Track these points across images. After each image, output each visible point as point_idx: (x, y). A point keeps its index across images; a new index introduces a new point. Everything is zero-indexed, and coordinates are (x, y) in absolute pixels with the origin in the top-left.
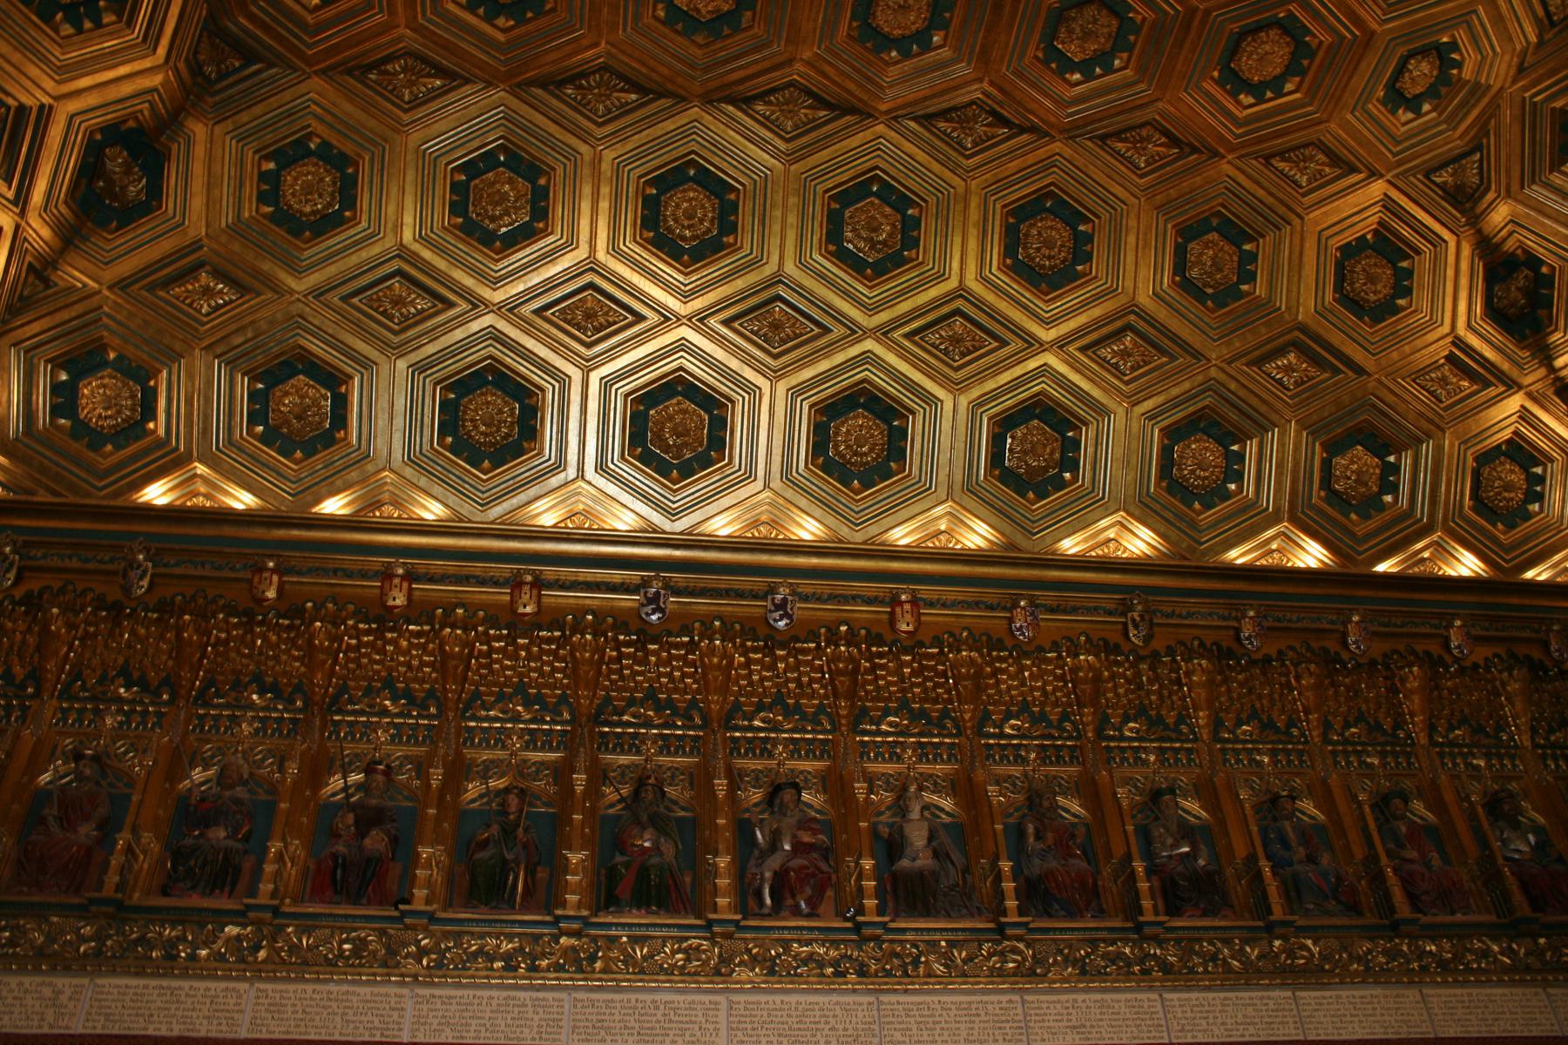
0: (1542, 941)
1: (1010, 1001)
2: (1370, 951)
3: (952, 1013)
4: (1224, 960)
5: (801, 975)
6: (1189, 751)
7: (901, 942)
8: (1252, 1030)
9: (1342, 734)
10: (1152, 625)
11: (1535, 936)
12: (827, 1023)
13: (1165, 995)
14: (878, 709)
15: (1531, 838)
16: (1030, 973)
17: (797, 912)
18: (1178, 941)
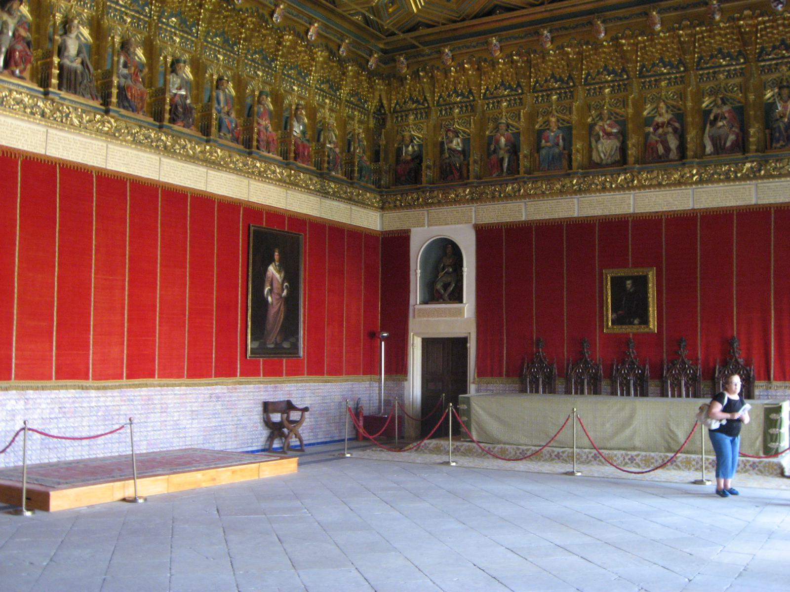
0: (293, 172)
1: (102, 146)
2: (137, 132)
4: (71, 118)
6: (193, 42)
8: (189, 183)
11: (291, 169)
12: (24, 137)
13: (162, 159)
16: (112, 135)
17: (13, 74)
18: (173, 136)
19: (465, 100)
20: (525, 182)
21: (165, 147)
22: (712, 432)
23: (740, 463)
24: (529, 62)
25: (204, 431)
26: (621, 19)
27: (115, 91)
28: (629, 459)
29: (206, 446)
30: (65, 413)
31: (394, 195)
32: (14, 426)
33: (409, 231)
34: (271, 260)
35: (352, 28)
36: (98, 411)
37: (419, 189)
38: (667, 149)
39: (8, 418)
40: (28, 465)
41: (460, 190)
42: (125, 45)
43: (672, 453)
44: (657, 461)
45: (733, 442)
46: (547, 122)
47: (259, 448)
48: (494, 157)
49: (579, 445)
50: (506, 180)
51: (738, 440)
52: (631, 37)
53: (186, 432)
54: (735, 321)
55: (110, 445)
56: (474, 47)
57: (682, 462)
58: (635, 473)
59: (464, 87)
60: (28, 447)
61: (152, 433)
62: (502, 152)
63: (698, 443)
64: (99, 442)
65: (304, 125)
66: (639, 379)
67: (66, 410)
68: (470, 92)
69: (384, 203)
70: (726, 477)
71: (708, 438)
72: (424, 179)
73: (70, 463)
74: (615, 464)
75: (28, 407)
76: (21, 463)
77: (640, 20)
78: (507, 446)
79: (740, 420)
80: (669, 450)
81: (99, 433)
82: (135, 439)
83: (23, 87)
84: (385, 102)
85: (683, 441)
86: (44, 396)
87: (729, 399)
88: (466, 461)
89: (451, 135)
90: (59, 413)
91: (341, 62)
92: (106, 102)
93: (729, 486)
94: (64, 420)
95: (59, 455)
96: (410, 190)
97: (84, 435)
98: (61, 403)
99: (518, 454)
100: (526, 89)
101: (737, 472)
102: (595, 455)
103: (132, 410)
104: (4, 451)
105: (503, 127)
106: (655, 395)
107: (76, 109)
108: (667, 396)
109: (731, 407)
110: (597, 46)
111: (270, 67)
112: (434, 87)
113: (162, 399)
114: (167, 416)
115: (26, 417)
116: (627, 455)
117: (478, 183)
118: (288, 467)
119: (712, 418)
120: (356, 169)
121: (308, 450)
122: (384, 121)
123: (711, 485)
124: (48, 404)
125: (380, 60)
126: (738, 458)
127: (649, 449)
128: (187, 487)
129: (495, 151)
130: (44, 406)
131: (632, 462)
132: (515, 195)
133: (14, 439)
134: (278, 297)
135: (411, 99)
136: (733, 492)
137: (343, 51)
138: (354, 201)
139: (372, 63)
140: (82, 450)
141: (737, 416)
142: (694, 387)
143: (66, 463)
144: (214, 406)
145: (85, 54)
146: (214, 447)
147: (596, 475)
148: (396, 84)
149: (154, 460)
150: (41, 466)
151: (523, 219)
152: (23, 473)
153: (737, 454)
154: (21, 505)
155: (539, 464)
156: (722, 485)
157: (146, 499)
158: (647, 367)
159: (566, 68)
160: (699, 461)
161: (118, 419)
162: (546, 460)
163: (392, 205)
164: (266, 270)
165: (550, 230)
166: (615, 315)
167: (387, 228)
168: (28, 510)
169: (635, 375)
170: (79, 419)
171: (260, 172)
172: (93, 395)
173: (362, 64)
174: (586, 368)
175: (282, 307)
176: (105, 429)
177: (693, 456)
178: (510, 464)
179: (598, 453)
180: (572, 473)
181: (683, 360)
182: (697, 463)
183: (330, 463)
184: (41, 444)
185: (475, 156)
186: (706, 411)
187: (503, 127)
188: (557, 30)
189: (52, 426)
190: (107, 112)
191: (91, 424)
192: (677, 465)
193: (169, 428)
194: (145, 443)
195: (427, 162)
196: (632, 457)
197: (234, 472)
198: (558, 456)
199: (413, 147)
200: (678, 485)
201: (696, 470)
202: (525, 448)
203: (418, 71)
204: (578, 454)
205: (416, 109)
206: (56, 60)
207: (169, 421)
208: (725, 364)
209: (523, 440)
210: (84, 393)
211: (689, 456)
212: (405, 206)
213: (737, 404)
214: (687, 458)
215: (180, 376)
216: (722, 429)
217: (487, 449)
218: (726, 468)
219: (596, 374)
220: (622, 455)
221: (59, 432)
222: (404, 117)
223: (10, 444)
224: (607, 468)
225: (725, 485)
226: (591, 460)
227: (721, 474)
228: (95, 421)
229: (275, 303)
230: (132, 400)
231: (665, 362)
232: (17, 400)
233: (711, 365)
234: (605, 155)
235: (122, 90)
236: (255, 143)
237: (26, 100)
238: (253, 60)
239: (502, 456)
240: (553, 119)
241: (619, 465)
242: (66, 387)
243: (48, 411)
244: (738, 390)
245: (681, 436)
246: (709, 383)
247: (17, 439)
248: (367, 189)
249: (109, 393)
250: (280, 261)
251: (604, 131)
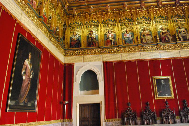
20: (121, 48)
31: (70, 51)
34: (27, 57)
38: (169, 39)
41: (97, 50)
46: (126, 31)
84: (67, 23)
129: (108, 38)
132: (117, 52)
134: (28, 77)
151: (121, 60)
163: (69, 54)
164: (24, 62)
165: (131, 64)
166: (159, 93)
167: (67, 62)
175: (29, 84)
187: (110, 31)
212: (74, 55)
229: (26, 80)
234: (148, 40)
250: (31, 59)
251: (146, 34)
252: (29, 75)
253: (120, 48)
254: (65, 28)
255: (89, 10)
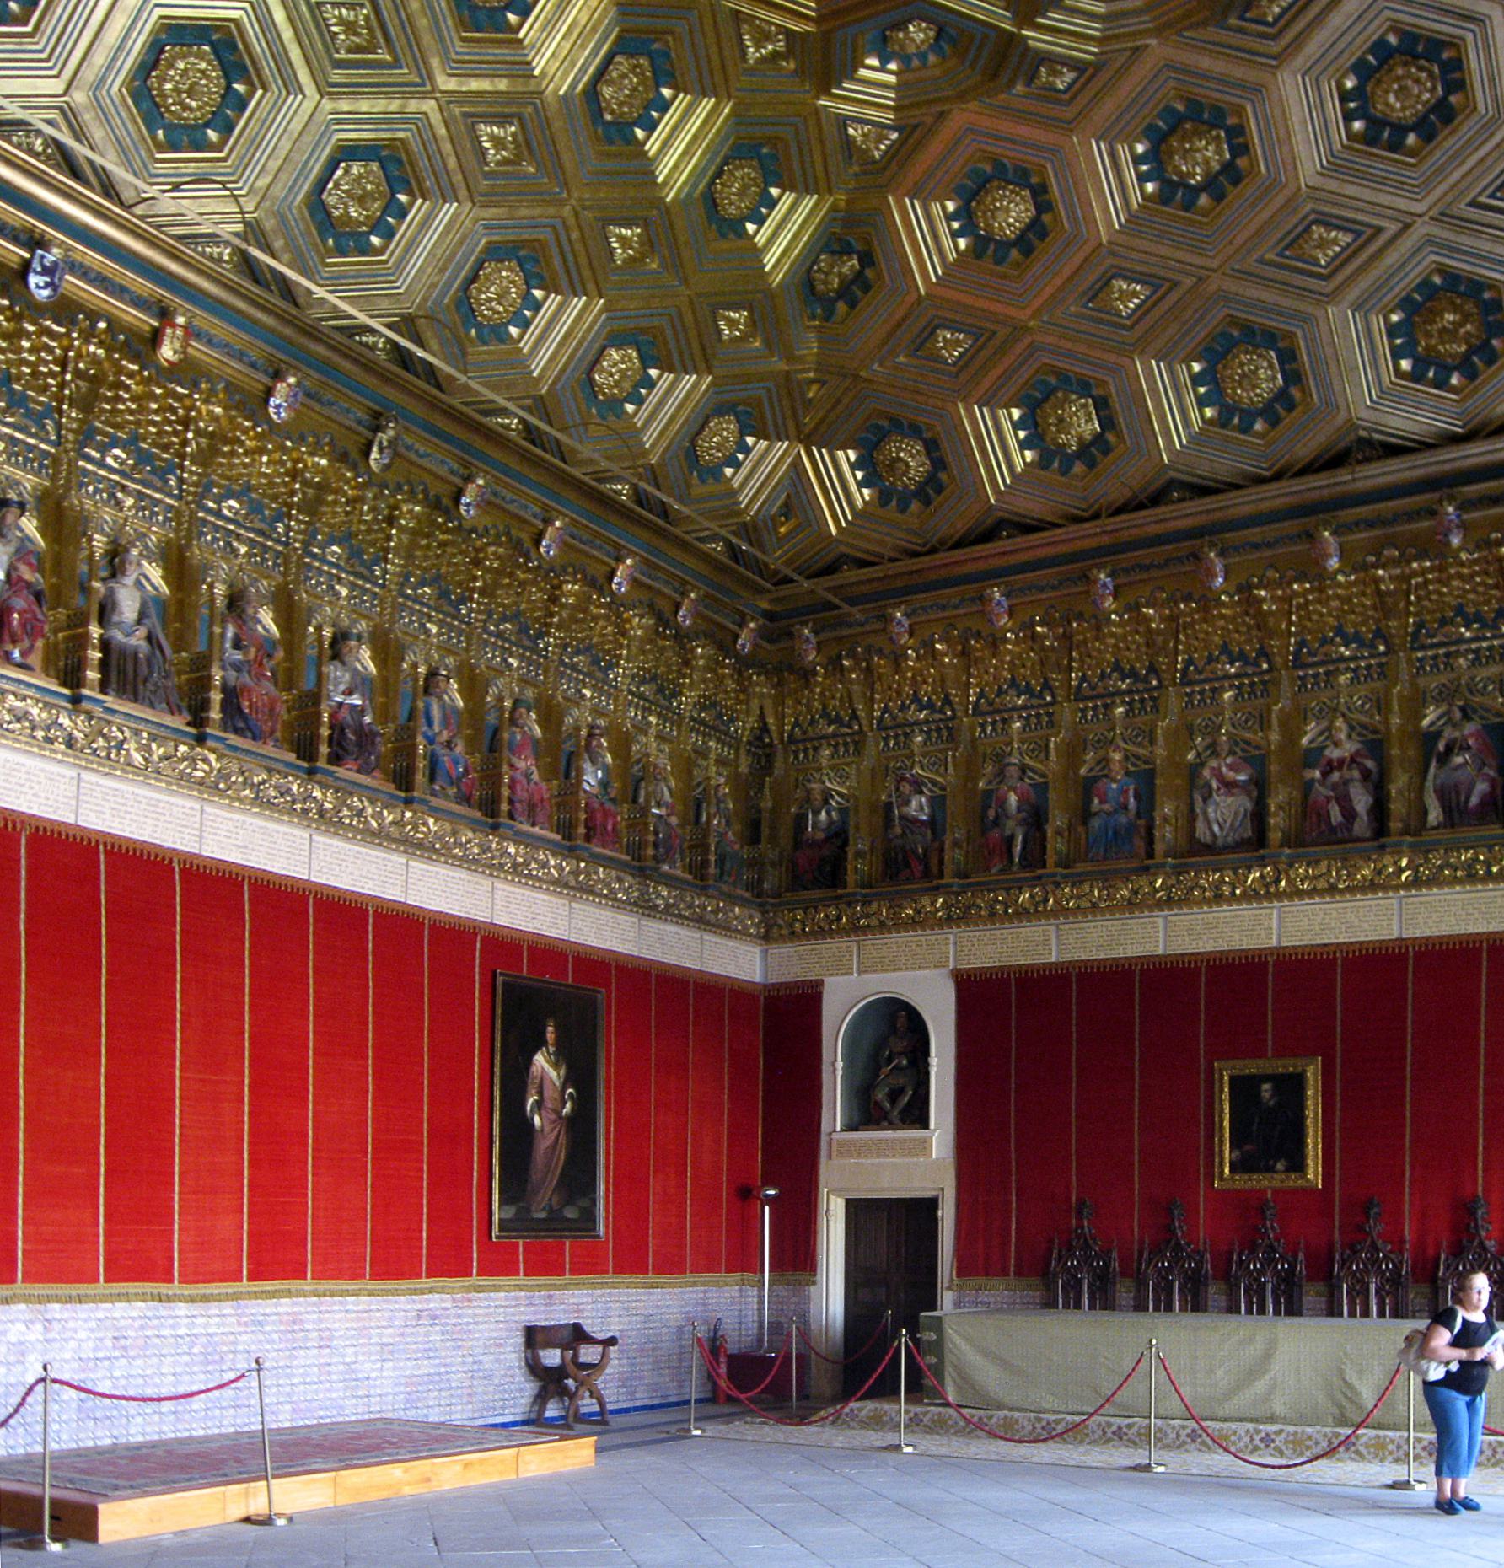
3: (143, 806)
5: (13, 732)
7: (109, 723)
9: (497, 626)
10: (396, 454)
11: (579, 860)
14: (106, 434)
15: (600, 774)
19: (937, 716)
21: (321, 813)
22: (1428, 1385)
23: (1485, 1447)
24: (1067, 637)
25: (406, 1385)
26: (1256, 546)
27: (216, 697)
28: (1261, 1440)
29: (411, 1415)
30: (125, 1348)
32: (23, 1374)
33: (819, 983)
35: (703, 569)
36: (192, 1345)
37: (840, 897)
39: (12, 1359)
40: (53, 1452)
41: (925, 901)
42: (236, 602)
43: (1348, 1427)
44: (1317, 1443)
45: (1471, 1405)
46: (1105, 761)
47: (518, 1418)
48: (995, 834)
49: (1161, 1412)
50: (1019, 880)
51: (1482, 1402)
52: (1279, 584)
53: (369, 1386)
54: (1480, 1165)
55: (217, 1412)
56: (956, 607)
57: (1367, 1446)
58: (1273, 1467)
59: (934, 692)
60: (53, 1415)
61: (302, 1387)
62: (1010, 824)
63: (1402, 1408)
64: (195, 1407)
65: (605, 768)
66: (1284, 1280)
67: (129, 1342)
68: (947, 701)
69: (769, 928)
70: (1455, 1475)
71: (1422, 1398)
72: (851, 878)
73: (139, 1447)
74: (1233, 1449)
75: (51, 1336)
76: (39, 1448)
77: (1299, 548)
78: (1017, 1414)
79: (1486, 1363)
80: (1343, 1421)
81: (195, 1388)
82: (266, 1400)
83: (29, 685)
84: (771, 721)
85: (1370, 1407)
86: (83, 1316)
87: (1464, 1321)
88: (934, 1444)
89: (906, 788)
90: (114, 1347)
91: (682, 638)
92: (198, 719)
93: (1462, 1493)
94: (123, 1361)
95: (115, 1433)
96: (820, 900)
97: (165, 1391)
98: (118, 1329)
99: (1039, 1430)
100: (1061, 694)
101: (1478, 1464)
102: (1194, 1431)
103: (260, 1342)
104: (6, 1421)
105: (1013, 771)
106: (1316, 1313)
107: (137, 733)
108: (1341, 1315)
109: (1468, 1337)
110: (1208, 602)
111: (535, 650)
112: (873, 691)
113: (321, 1321)
114: (331, 1355)
115: (47, 1358)
116: (1258, 1432)
117: (962, 886)
118: (575, 1455)
119: (1431, 1360)
120: (712, 858)
121: (616, 1421)
122: (770, 758)
123: (1425, 1491)
124: (92, 1330)
125: (761, 633)
126: (1481, 1438)
127: (1301, 1420)
128: (374, 1496)
129: (996, 822)
130: (82, 1335)
131: (1267, 1446)
133: (24, 1399)
135: (825, 714)
136: (1469, 1505)
137: (684, 617)
138: (708, 923)
139: (745, 641)
140: (162, 1422)
141: (1480, 1355)
142: (1396, 1297)
143: (129, 1447)
144: (427, 1335)
145: (154, 620)
146: (426, 1416)
147: (1195, 1471)
148: (793, 683)
149: (307, 1441)
150: (79, 1453)
152: (44, 1468)
153: (1480, 1430)
154: (42, 1532)
155: (1081, 1449)
156: (1448, 1493)
157: (290, 1519)
158: (1301, 1256)
159: (1144, 649)
160: (1402, 1442)
161: (233, 1361)
162: (1094, 1442)
168: (55, 1540)
169: (1277, 1273)
170: (155, 1360)
171: (515, 865)
172: (181, 1313)
173: (724, 643)
174: (1177, 1260)
176: (205, 1383)
177: (1390, 1434)
178: (1023, 1450)
179: (1201, 1428)
180: (1147, 1468)
181: (1373, 1242)
182: (1399, 1447)
183: (660, 1447)
184: (80, 1409)
185: (956, 832)
186: (1419, 1345)
187: (1013, 771)
188: (1126, 571)
189: (99, 1375)
190: (201, 739)
191: (179, 1370)
192: (1357, 1452)
193: (334, 1377)
194: (288, 1407)
195: (859, 843)
196: (1268, 1435)
197: (466, 1466)
198: (1119, 1433)
199: (828, 813)
200: (1359, 1491)
201: (1397, 1460)
202: (1053, 1417)
203: (839, 657)
204: (1159, 1430)
205: (834, 735)
206: (95, 631)
207: (336, 1364)
208: (1457, 1251)
209: (1050, 1402)
210: (163, 1310)
211: (1381, 1433)
212: (812, 931)
213: (1481, 1330)
214: (1378, 1437)
215: (357, 1275)
216: (1450, 1381)
217: (976, 1419)
218: (1457, 1457)
219: (1197, 1270)
220: (1248, 1431)
221: (115, 1387)
222: (811, 752)
223: (16, 1411)
224: (1216, 1456)
225: (1454, 1490)
226: (1184, 1442)
227: (1445, 1468)
228: (187, 1364)
230: (260, 1323)
231: (1338, 1246)
232: (28, 1323)
233: (1431, 1252)
235: (231, 696)
236: (504, 807)
237: (35, 711)
238: (500, 635)
239: (1007, 1433)
240: (1117, 756)
241: (1241, 1451)
242: (127, 1298)
243: (91, 1344)
244: (1484, 1303)
245: (1368, 1395)
246: (1426, 1289)
247: (29, 1399)
248: (733, 900)
249: (214, 1308)
252: (558, 1105)
253: (1050, 888)
254: (768, 756)
255: (884, 630)
